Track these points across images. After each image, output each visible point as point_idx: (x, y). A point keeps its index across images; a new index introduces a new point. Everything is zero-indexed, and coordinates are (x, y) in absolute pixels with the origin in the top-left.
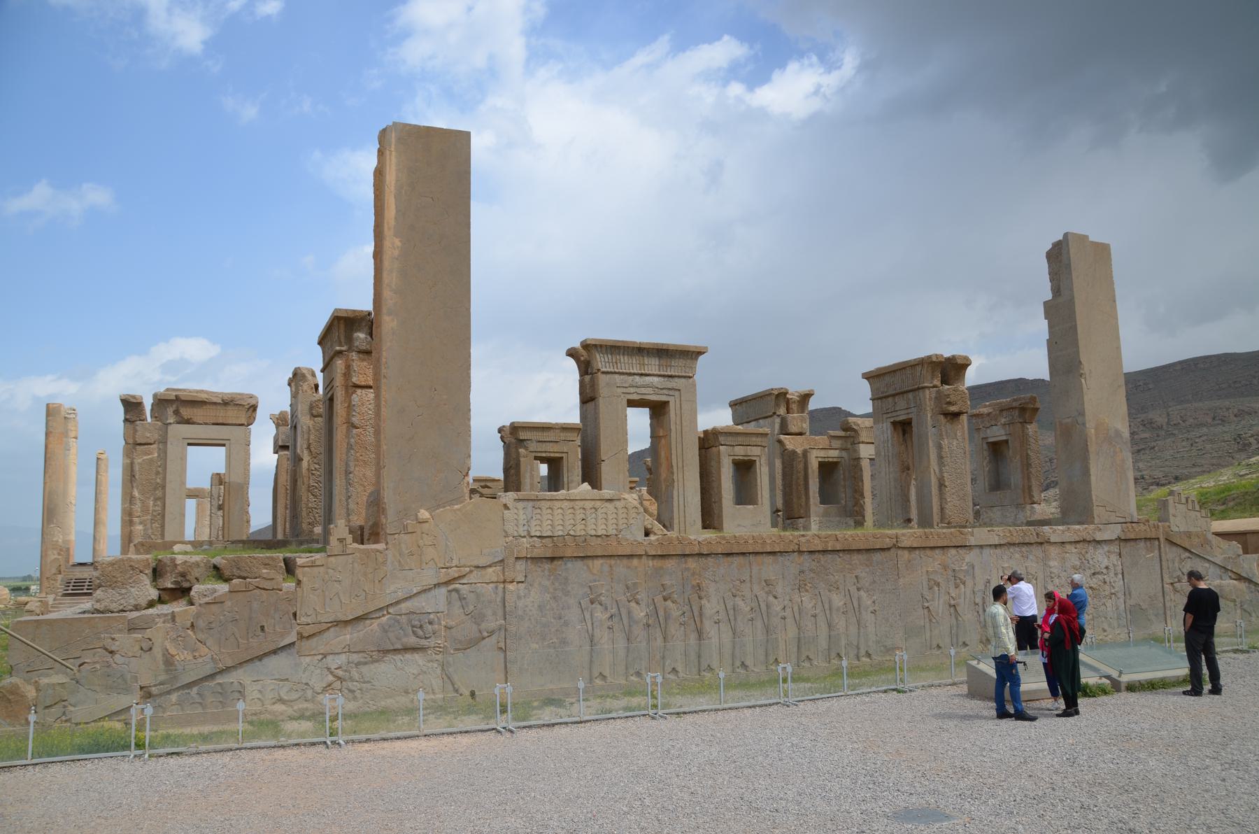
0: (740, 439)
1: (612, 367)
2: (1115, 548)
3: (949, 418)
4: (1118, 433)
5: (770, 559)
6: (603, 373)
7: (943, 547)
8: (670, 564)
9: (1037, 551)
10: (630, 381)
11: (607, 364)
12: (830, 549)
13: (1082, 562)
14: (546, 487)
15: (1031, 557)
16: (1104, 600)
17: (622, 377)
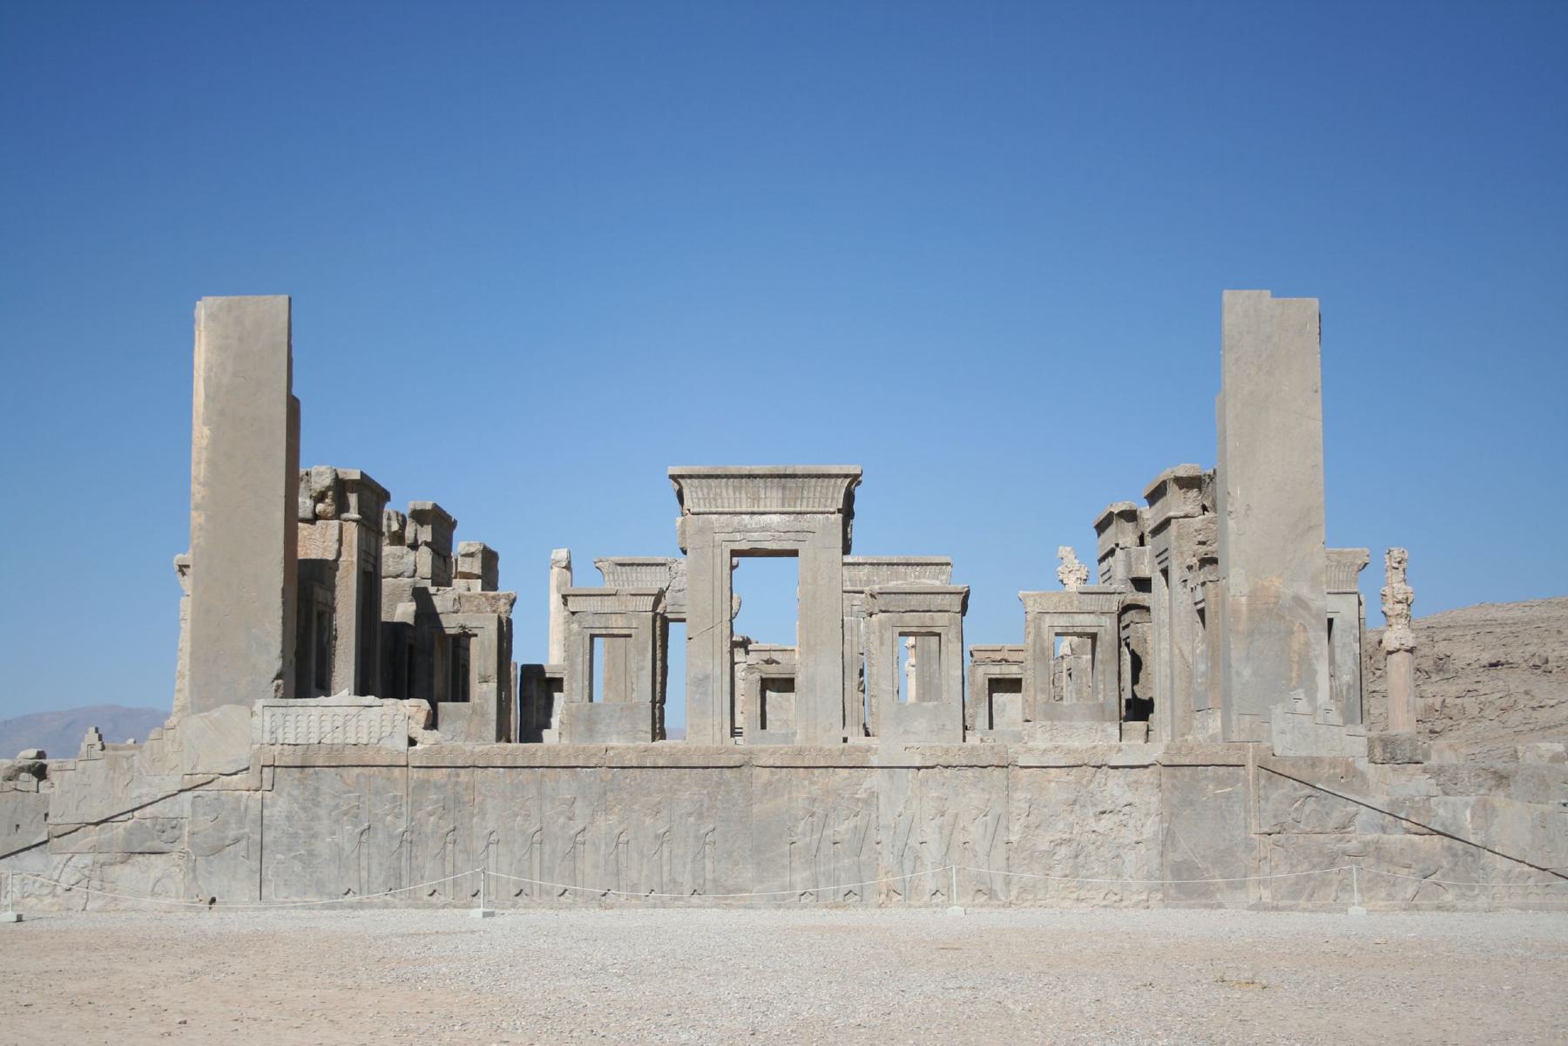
0: (914, 601)
1: (708, 505)
6: (693, 514)
10: (736, 523)
11: (701, 501)
14: (293, 690)
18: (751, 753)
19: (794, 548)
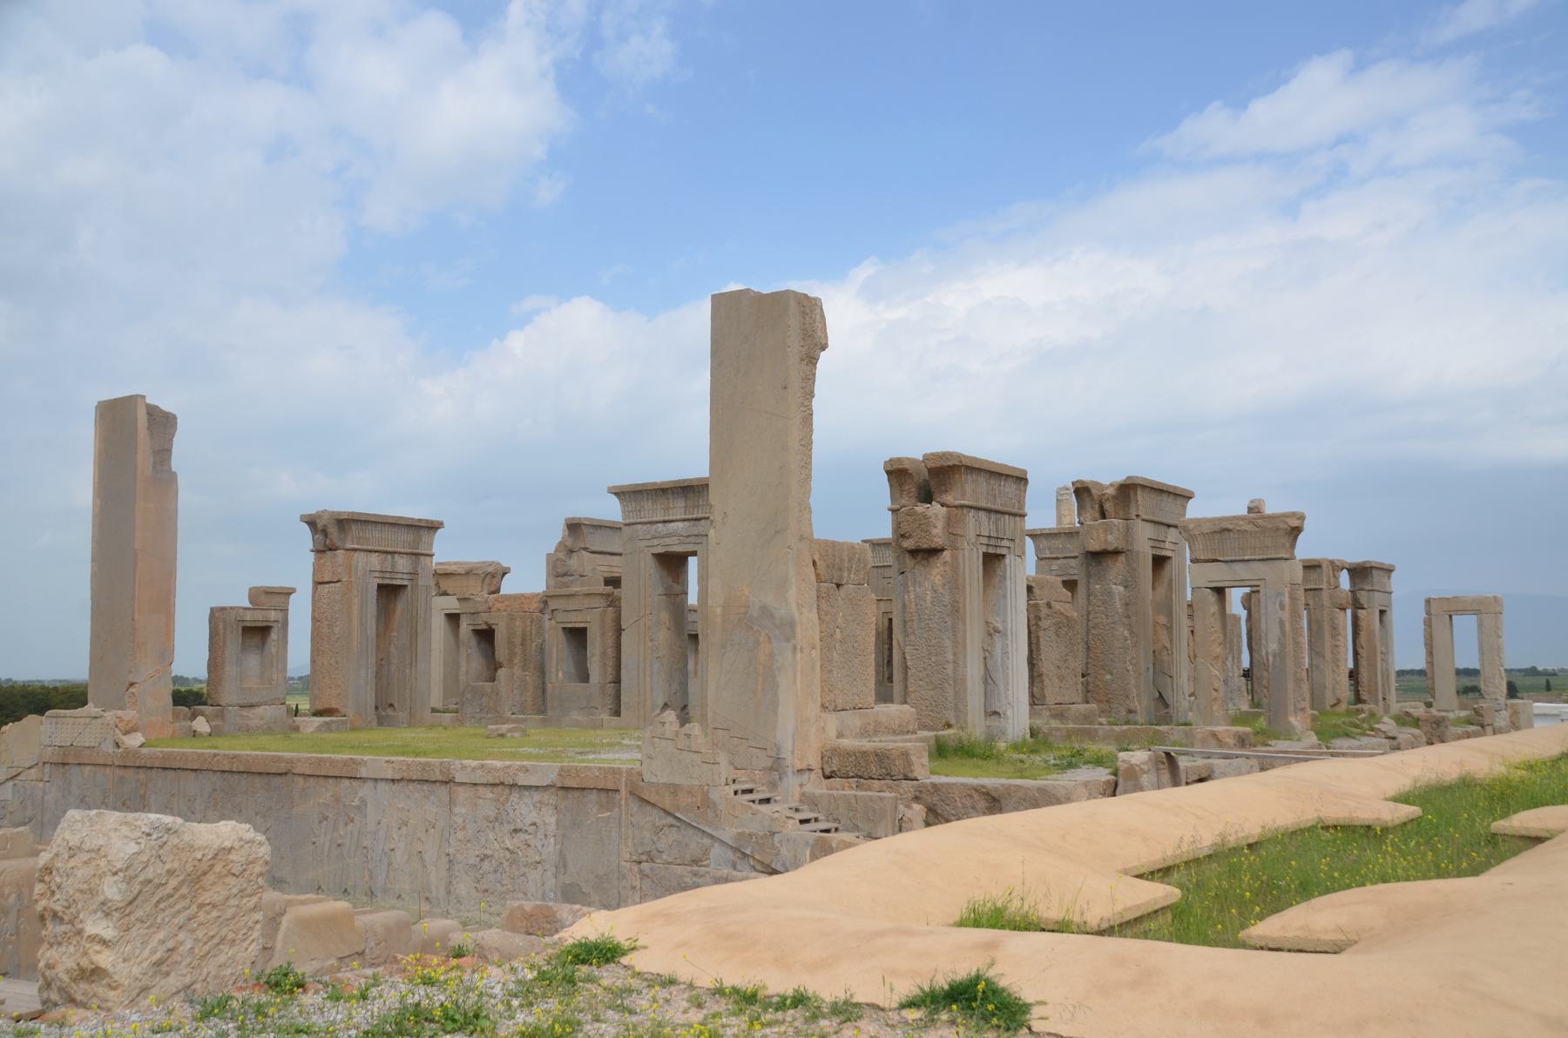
2: (549, 798)
3: (919, 558)
4: (766, 611)
5: (192, 775)
7: (336, 777)
8: (129, 773)
9: (442, 792)
12: (234, 770)
13: (500, 813)
15: (432, 798)
16: (526, 870)
17: (645, 527)
18: (292, 762)
19: (693, 550)
